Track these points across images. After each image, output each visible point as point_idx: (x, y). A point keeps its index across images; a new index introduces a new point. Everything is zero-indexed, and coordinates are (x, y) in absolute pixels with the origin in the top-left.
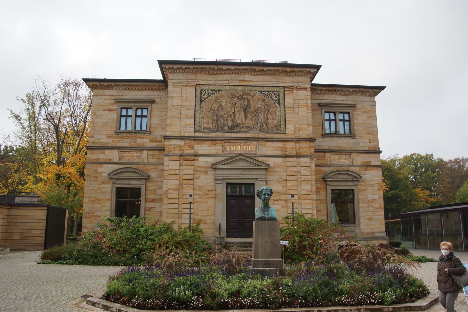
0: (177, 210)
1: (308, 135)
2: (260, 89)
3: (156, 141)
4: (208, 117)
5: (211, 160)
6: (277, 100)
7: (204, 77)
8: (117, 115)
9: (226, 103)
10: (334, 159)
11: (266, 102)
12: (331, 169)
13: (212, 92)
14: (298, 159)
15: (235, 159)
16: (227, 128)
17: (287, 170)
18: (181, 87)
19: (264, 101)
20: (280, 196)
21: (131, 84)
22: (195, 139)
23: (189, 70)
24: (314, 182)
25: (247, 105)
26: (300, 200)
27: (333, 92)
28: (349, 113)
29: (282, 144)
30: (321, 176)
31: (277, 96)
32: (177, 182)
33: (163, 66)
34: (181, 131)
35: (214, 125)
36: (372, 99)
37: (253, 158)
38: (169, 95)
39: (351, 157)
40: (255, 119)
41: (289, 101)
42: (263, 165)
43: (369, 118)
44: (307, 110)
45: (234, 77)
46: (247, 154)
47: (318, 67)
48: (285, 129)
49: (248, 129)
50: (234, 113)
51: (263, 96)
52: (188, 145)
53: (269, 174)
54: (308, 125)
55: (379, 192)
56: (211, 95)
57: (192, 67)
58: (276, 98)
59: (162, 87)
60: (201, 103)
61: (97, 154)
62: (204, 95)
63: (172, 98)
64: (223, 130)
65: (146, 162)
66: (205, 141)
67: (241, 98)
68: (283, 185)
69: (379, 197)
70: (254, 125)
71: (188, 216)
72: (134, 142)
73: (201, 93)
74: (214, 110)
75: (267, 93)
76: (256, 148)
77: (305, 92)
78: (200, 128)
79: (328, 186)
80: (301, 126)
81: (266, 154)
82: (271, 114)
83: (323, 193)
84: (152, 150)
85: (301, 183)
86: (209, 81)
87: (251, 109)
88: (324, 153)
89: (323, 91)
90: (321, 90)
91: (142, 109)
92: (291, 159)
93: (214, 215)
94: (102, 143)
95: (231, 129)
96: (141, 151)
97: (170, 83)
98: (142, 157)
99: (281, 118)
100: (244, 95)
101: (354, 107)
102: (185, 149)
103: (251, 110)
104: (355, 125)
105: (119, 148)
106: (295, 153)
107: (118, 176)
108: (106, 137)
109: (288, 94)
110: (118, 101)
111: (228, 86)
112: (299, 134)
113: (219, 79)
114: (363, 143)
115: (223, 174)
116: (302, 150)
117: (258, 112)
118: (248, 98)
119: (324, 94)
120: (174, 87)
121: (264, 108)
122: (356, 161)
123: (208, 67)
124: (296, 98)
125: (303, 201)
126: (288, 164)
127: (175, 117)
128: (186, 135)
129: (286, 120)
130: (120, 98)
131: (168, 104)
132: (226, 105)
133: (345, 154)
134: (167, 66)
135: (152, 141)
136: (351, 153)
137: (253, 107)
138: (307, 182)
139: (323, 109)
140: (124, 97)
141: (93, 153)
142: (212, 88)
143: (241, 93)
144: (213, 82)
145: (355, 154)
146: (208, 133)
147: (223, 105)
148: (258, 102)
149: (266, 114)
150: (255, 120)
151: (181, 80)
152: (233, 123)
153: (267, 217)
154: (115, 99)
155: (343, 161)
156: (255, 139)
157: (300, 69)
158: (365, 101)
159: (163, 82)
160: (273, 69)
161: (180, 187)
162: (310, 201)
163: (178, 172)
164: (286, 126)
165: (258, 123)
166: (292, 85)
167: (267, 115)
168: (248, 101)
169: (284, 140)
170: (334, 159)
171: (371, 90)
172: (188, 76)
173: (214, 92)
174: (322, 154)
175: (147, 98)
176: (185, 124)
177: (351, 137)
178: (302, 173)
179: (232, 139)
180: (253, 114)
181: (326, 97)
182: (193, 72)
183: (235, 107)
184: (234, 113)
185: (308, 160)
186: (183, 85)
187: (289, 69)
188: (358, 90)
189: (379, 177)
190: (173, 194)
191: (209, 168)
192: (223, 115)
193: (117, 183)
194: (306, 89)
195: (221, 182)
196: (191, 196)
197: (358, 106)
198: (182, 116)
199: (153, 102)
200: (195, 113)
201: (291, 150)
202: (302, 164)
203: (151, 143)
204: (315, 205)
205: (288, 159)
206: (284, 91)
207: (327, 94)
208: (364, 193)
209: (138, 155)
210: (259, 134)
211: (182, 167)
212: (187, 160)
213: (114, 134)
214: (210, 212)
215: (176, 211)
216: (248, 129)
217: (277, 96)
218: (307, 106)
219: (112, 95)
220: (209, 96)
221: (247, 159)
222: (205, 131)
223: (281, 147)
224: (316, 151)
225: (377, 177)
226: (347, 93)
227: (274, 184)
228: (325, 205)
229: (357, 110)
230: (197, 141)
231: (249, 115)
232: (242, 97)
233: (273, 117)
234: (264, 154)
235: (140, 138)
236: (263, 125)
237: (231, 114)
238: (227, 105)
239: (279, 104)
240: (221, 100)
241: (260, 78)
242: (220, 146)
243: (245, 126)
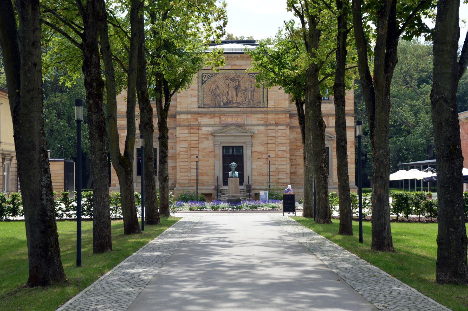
0: (187, 166)
5: (210, 129)
9: (222, 84)
13: (210, 75)
17: (268, 135)
19: (251, 81)
20: (262, 155)
22: (198, 113)
24: (288, 145)
32: (186, 146)
35: (213, 102)
50: (228, 92)
52: (194, 118)
53: (254, 139)
60: (202, 85)
62: (205, 78)
64: (219, 106)
67: (233, 79)
71: (195, 171)
73: (202, 77)
74: (213, 90)
76: (245, 119)
80: (279, 101)
82: (256, 92)
93: (214, 169)
95: (226, 105)
103: (241, 89)
106: (274, 122)
116: (279, 120)
117: (246, 90)
121: (251, 87)
125: (280, 159)
126: (269, 131)
128: (192, 110)
137: (242, 86)
143: (233, 76)
146: (208, 109)
147: (220, 86)
148: (246, 83)
153: (233, 176)
161: (189, 150)
162: (285, 159)
163: (187, 139)
165: (246, 100)
168: (239, 82)
180: (242, 93)
184: (228, 92)
190: (183, 155)
191: (209, 135)
196: (197, 157)
198: (188, 95)
204: (289, 162)
205: (269, 128)
211: (189, 135)
212: (193, 129)
214: (211, 168)
215: (187, 167)
222: (206, 107)
223: (263, 118)
233: (258, 94)
236: (250, 101)
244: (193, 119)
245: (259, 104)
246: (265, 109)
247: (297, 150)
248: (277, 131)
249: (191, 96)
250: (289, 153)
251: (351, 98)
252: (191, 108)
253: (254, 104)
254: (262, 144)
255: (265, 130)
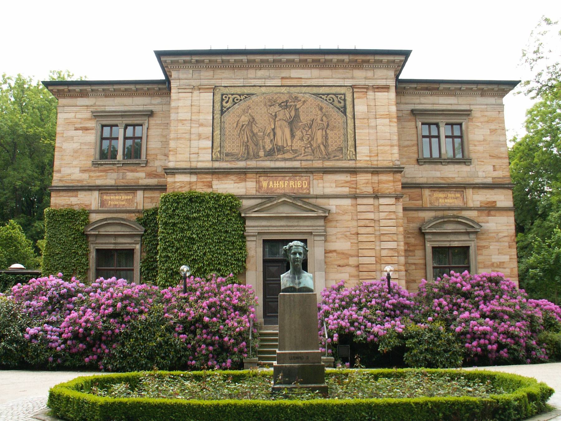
1: (392, 161)
2: (315, 90)
3: (156, 176)
4: (233, 137)
6: (342, 108)
7: (227, 73)
8: (96, 137)
10: (437, 199)
11: (324, 110)
12: (432, 214)
13: (239, 97)
14: (376, 201)
15: (275, 202)
16: (263, 153)
18: (190, 91)
19: (321, 109)
20: (348, 258)
21: (116, 87)
23: (202, 65)
24: (401, 237)
25: (294, 117)
26: (378, 265)
27: (435, 92)
28: (460, 124)
29: (350, 177)
30: (414, 226)
31: (342, 101)
33: (163, 59)
34: (191, 160)
36: (498, 101)
37: (304, 200)
38: (173, 104)
39: (465, 194)
40: (307, 138)
41: (361, 107)
42: (321, 212)
43: (493, 131)
44: (390, 121)
45: (272, 72)
46: (294, 193)
47: (406, 54)
48: (354, 153)
49: (296, 155)
51: (318, 101)
53: (329, 224)
54: (392, 146)
55: (509, 250)
56: (237, 101)
57: (206, 59)
58: (340, 104)
59: (164, 91)
61: (65, 198)
63: (177, 108)
64: (256, 156)
65: (142, 208)
66: (230, 175)
67: (285, 105)
68: (352, 241)
69: (510, 259)
70: (305, 148)
72: (123, 179)
73: (222, 100)
74: (243, 126)
75: (326, 97)
76: (309, 184)
77: (386, 93)
78: (220, 155)
79: (428, 241)
80: (379, 148)
81: (325, 193)
82: (332, 130)
83: (419, 253)
84: (150, 189)
85: (380, 237)
86: (234, 80)
87: (301, 122)
88: (420, 189)
89: (419, 90)
90: (416, 88)
91: (134, 126)
92: (365, 201)
94: (74, 181)
95: (270, 154)
96: (134, 192)
97: (174, 84)
98: (135, 201)
99: (349, 136)
100: (290, 101)
101: (469, 115)
102: (198, 187)
103: (300, 124)
104: (470, 142)
105: (101, 189)
107: (99, 232)
108: (80, 171)
109: (359, 98)
110: (96, 115)
111: (264, 88)
112: (378, 161)
113: (250, 76)
114: (484, 172)
115: (257, 226)
117: (311, 128)
118: (296, 106)
119: (420, 95)
120: (180, 91)
121: (322, 120)
122: (473, 201)
123: (232, 58)
124: (372, 103)
126: (360, 208)
127: (182, 138)
128: (200, 165)
129: (356, 138)
130: (100, 109)
131: (171, 118)
132: (262, 116)
133: (454, 190)
134: (169, 59)
135: (150, 175)
136: (465, 188)
137: (304, 119)
138: (389, 237)
139: (419, 119)
140: (106, 107)
141: (60, 196)
142: (239, 90)
143: (285, 98)
144: (240, 82)
145: (471, 190)
149: (324, 131)
150: (308, 140)
151: (190, 79)
152: (273, 146)
154: (92, 112)
155: (451, 201)
156: (307, 170)
157: (378, 58)
158: (487, 105)
159: (166, 83)
160: (335, 58)
164: (357, 148)
165: (311, 145)
166: (366, 82)
167: (326, 131)
168: (297, 110)
169: (354, 171)
170: (437, 199)
171: (495, 87)
172: (202, 74)
173: (242, 97)
174: (418, 190)
175: (141, 108)
176: (197, 149)
177: (465, 162)
178: (383, 223)
179: (271, 170)
180: (304, 131)
181: (423, 100)
182: (210, 67)
183: (275, 120)
185: (392, 201)
186: (194, 88)
187: (360, 58)
188: (474, 87)
189: (510, 226)
192: (257, 133)
193: (97, 241)
194: (388, 88)
195: (254, 239)
197: (476, 114)
199: (151, 114)
200: (213, 131)
201: (365, 185)
202: (382, 208)
203: (149, 178)
204: (403, 273)
205: (360, 201)
206: (353, 93)
207: (424, 95)
208: (485, 252)
209: (129, 197)
210: (314, 161)
213: (91, 165)
216: (296, 155)
217: (342, 101)
218: (389, 116)
219: (87, 106)
220: (234, 104)
221: (295, 202)
224: (405, 186)
225: (506, 226)
226: (458, 92)
227: (338, 240)
228: (423, 271)
229: (474, 120)
230: (217, 175)
231: (298, 131)
232: (287, 104)
233: (335, 134)
234: (322, 193)
235: (132, 171)
236: (319, 147)
237: (268, 132)
238: (263, 117)
239: (345, 113)
240: (253, 109)
241: (316, 72)
242: (252, 181)
243: (292, 150)
244: (201, 184)
245: (338, 154)
246: (351, 164)
247: (410, 253)
248: (377, 209)
249: (197, 138)
250: (403, 254)
251: (504, 156)
252: (198, 161)
253: (328, 154)
254: (346, 236)
255: (352, 205)
